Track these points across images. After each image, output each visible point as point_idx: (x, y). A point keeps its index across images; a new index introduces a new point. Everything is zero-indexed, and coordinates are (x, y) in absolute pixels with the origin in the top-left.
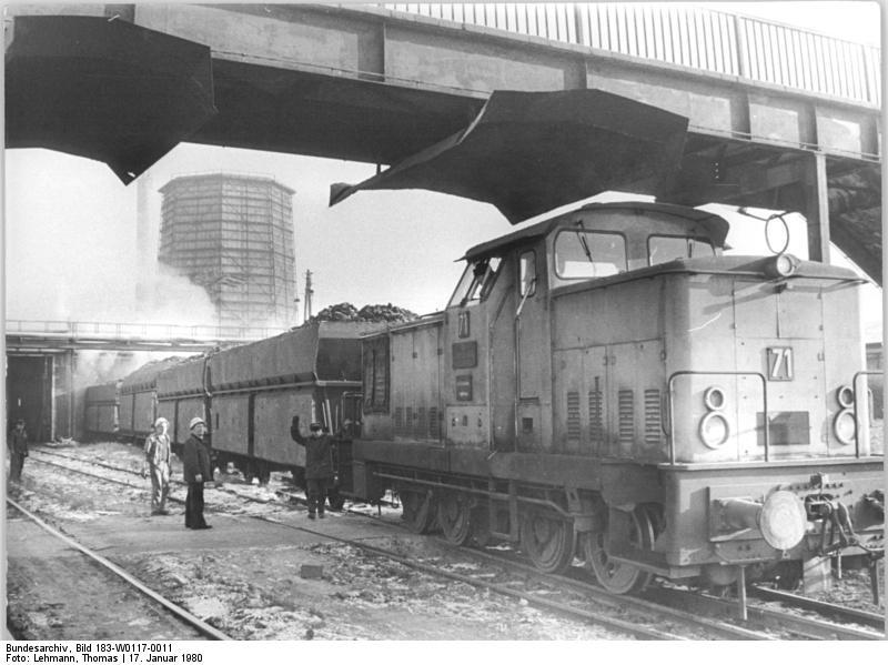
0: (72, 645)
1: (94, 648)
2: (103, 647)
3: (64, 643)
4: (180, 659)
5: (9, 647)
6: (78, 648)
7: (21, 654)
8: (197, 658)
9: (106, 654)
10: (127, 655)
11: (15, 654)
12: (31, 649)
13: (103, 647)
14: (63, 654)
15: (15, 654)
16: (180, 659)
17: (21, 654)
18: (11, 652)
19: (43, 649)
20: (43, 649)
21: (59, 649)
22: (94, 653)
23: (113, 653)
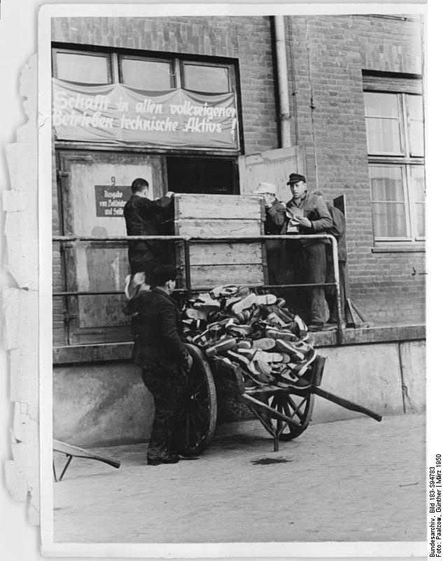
0: (430, 516)
1: (432, 502)
2: (432, 496)
3: (429, 520)
4: (439, 469)
5: (432, 556)
6: (432, 512)
7: (436, 547)
8: (438, 457)
9: (436, 495)
10: (436, 484)
11: (436, 551)
12: (433, 541)
13: (433, 496)
14: (436, 521)
15: (436, 551)
16: (439, 469)
17: (436, 547)
18: (435, 554)
19: (433, 534)
20: (433, 534)
21: (433, 523)
22: (435, 502)
23: (436, 492)
